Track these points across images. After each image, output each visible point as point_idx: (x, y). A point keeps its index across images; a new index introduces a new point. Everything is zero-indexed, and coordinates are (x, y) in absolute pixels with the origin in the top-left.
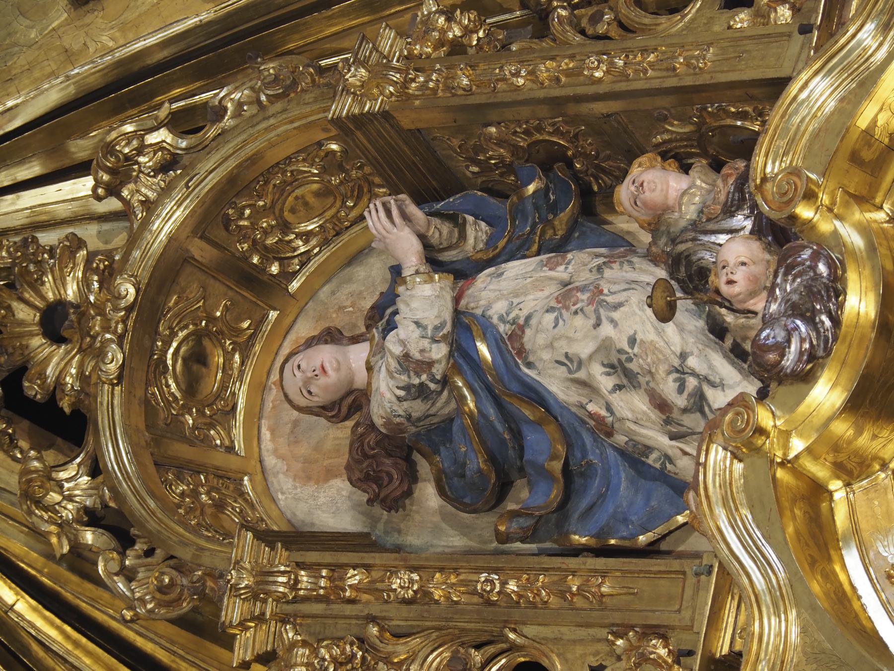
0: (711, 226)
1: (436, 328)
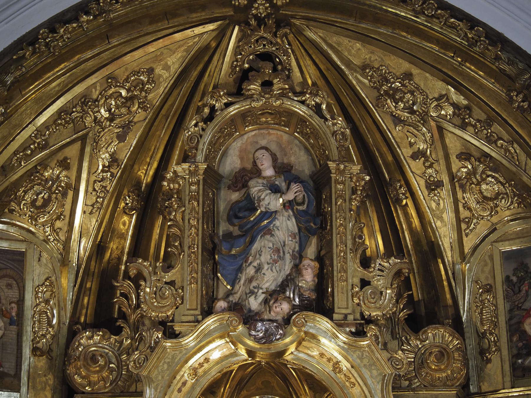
0: (296, 291)
1: (269, 209)
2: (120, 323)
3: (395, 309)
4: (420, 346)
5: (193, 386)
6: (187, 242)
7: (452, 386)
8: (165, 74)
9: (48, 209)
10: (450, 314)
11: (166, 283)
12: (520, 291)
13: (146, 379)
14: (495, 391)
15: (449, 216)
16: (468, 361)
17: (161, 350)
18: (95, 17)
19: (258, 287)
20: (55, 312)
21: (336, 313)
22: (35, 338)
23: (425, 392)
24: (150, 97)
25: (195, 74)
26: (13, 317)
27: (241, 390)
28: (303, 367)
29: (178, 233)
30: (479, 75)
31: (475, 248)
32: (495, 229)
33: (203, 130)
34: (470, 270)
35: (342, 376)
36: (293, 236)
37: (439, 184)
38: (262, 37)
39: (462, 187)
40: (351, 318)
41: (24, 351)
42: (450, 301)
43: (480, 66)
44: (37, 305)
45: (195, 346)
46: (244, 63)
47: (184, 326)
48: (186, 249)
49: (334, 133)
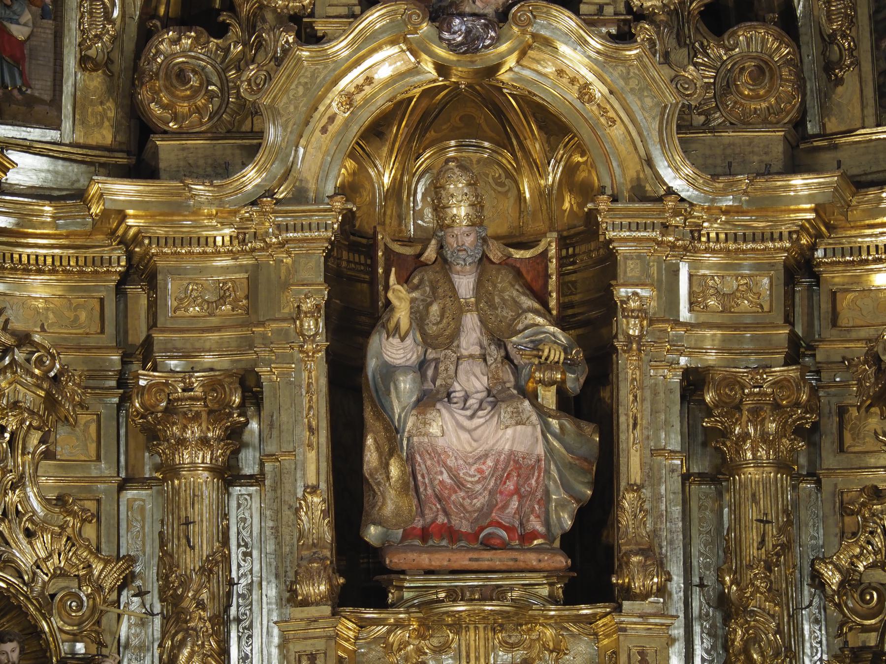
2: (224, 17)
4: (725, 58)
5: (347, 124)
7: (778, 123)
10: (776, 4)
13: (269, 111)
14: (849, 132)
16: (805, 82)
17: (292, 63)
21: (585, 3)
22: (84, 40)
23: (731, 134)
26: (46, 5)
27: (427, 130)
28: (530, 92)
35: (594, 108)
40: (609, 10)
41: (66, 62)
45: (350, 56)
47: (331, 23)
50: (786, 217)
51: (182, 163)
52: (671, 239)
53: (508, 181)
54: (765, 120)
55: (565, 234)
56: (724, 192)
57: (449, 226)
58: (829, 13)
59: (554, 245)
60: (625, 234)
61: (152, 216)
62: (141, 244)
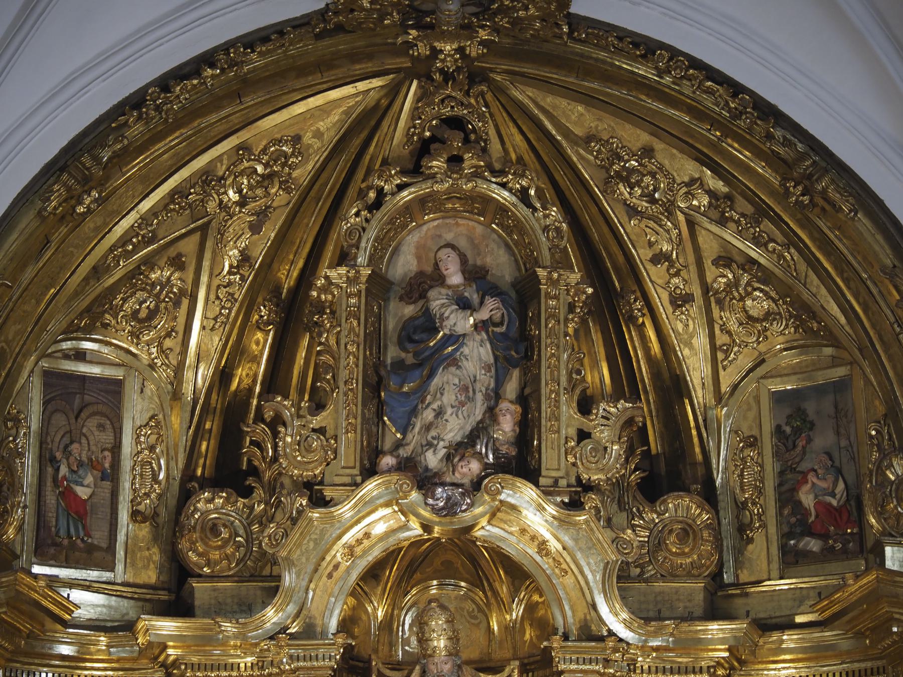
0: (490, 445)
1: (454, 331)
3: (623, 471)
4: (657, 521)
5: (348, 570)
6: (343, 374)
8: (316, 143)
9: (155, 322)
10: (699, 474)
11: (314, 430)
12: (795, 446)
13: (285, 562)
14: (758, 583)
15: (701, 341)
16: (722, 542)
17: (305, 524)
18: (223, 70)
19: (438, 438)
20: (162, 462)
21: (544, 477)
22: (135, 497)
23: (661, 584)
24: (295, 174)
25: (357, 142)
26: (105, 469)
27: (415, 571)
28: (498, 546)
29: (331, 362)
30: (743, 156)
31: (735, 387)
32: (763, 361)
33: (367, 221)
34: (728, 416)
35: (551, 560)
36: (487, 368)
37: (688, 299)
38: (449, 96)
39: (719, 302)
40: (563, 483)
41: (120, 516)
42: (699, 457)
43: (746, 144)
44: (139, 453)
45: (352, 517)
46: (424, 131)
47: (337, 490)
48: (341, 384)
49: (546, 229)
50: (705, 655)
51: (213, 602)
52: (611, 671)
53: (480, 615)
54: (689, 574)
55: (526, 661)
56: (656, 634)
57: (430, 656)
58: (742, 483)
59: (516, 671)
60: (573, 667)
61: (189, 647)
62: (179, 668)
